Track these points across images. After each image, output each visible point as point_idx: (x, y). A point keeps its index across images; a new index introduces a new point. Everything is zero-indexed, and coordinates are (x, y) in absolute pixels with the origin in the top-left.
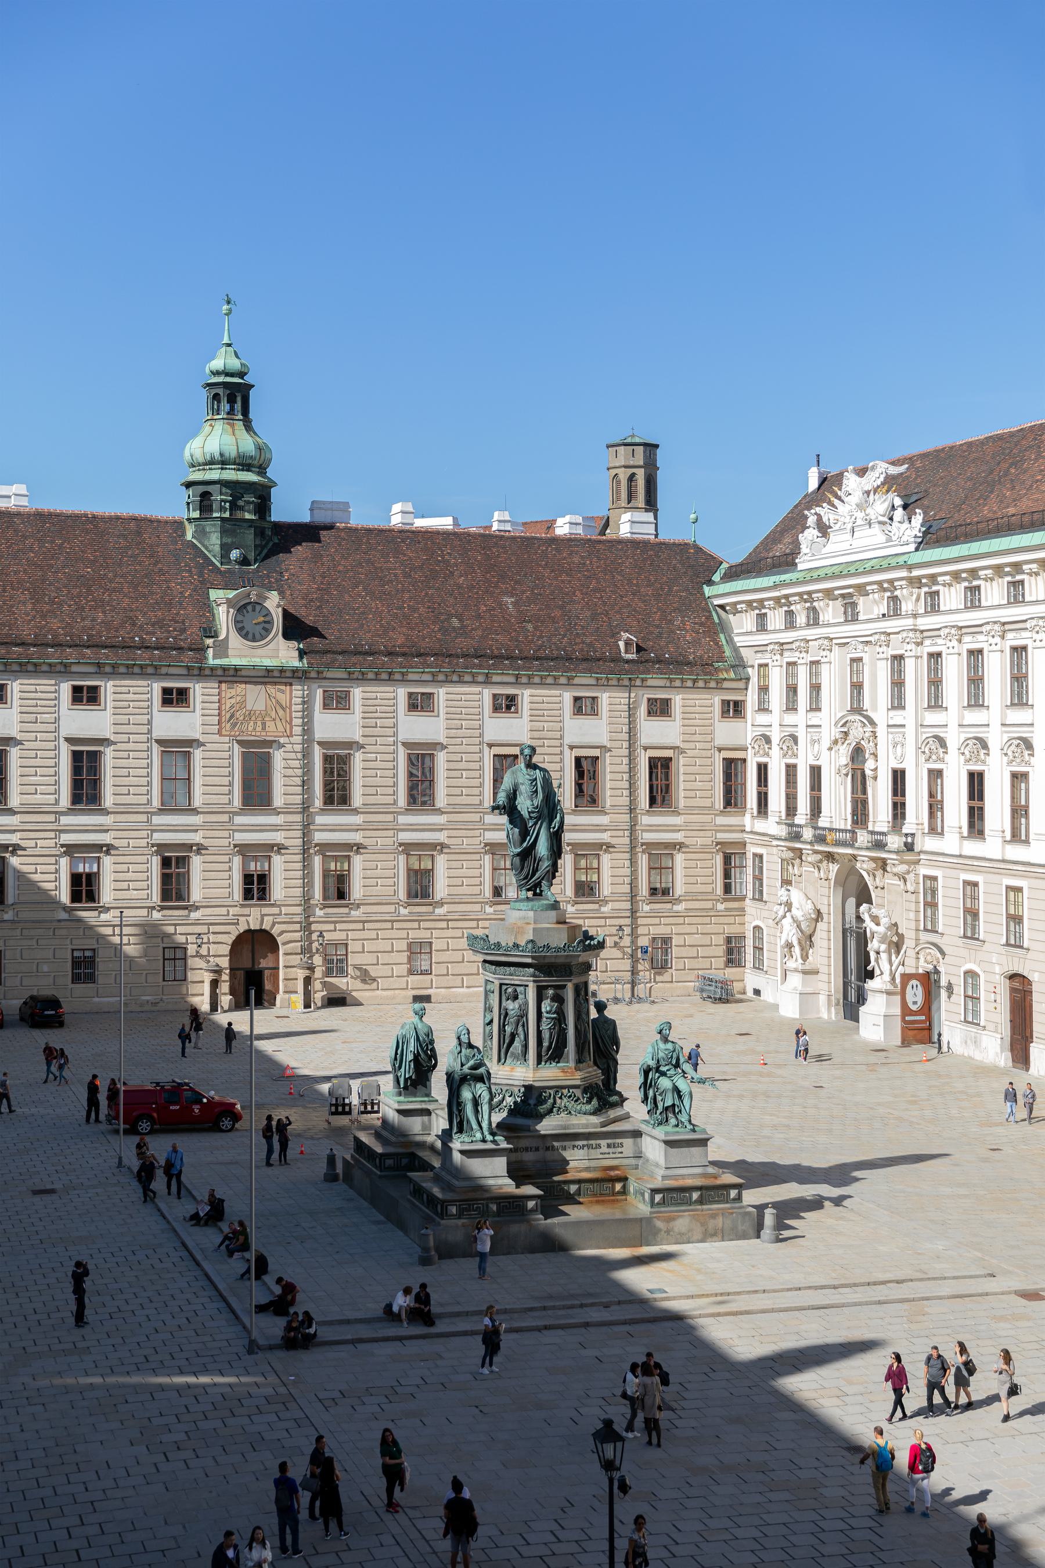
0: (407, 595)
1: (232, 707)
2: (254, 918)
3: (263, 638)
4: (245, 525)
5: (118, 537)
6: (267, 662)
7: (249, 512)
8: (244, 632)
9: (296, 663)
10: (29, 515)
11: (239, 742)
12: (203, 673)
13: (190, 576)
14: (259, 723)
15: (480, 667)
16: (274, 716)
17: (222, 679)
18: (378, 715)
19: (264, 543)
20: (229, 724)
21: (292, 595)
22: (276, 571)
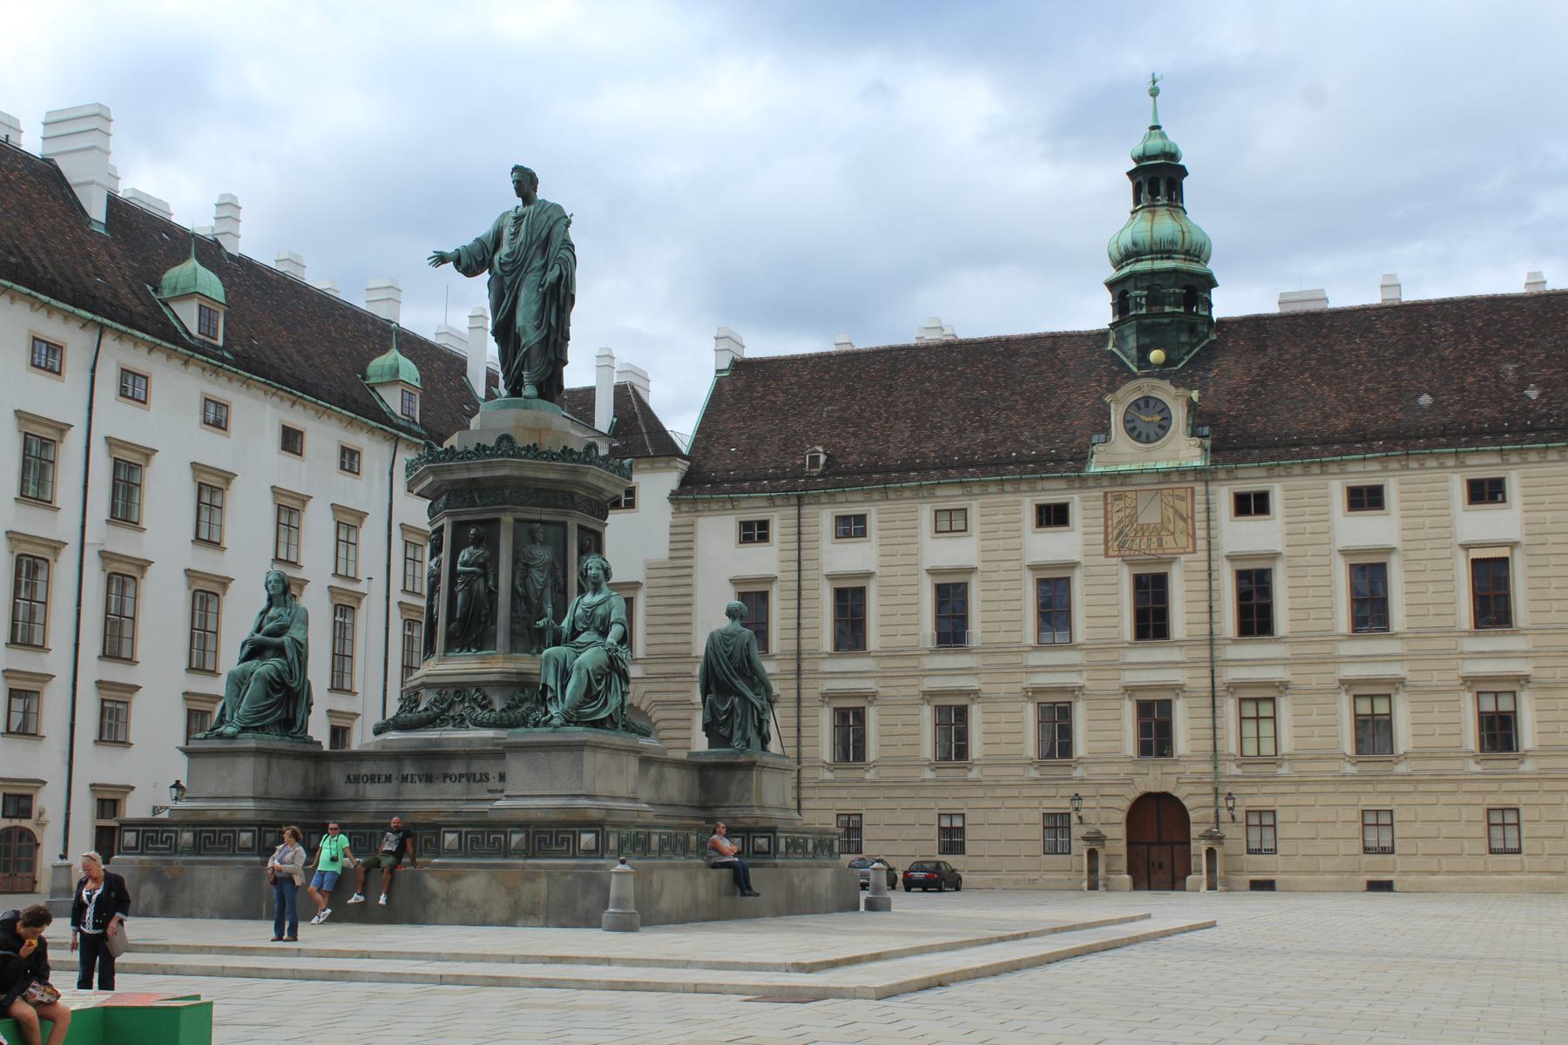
0: (1366, 377)
1: (1120, 522)
2: (1155, 778)
3: (1159, 438)
4: (1166, 320)
5: (1028, 355)
6: (1161, 465)
7: (1170, 305)
8: (1136, 433)
9: (1198, 463)
10: (938, 346)
11: (1131, 564)
12: (1081, 480)
13: (1098, 386)
14: (1154, 539)
15: (1446, 446)
16: (1172, 530)
17: (1106, 490)
18: (1307, 518)
19: (1195, 340)
20: (1117, 543)
21: (1215, 391)
22: (1204, 369)
